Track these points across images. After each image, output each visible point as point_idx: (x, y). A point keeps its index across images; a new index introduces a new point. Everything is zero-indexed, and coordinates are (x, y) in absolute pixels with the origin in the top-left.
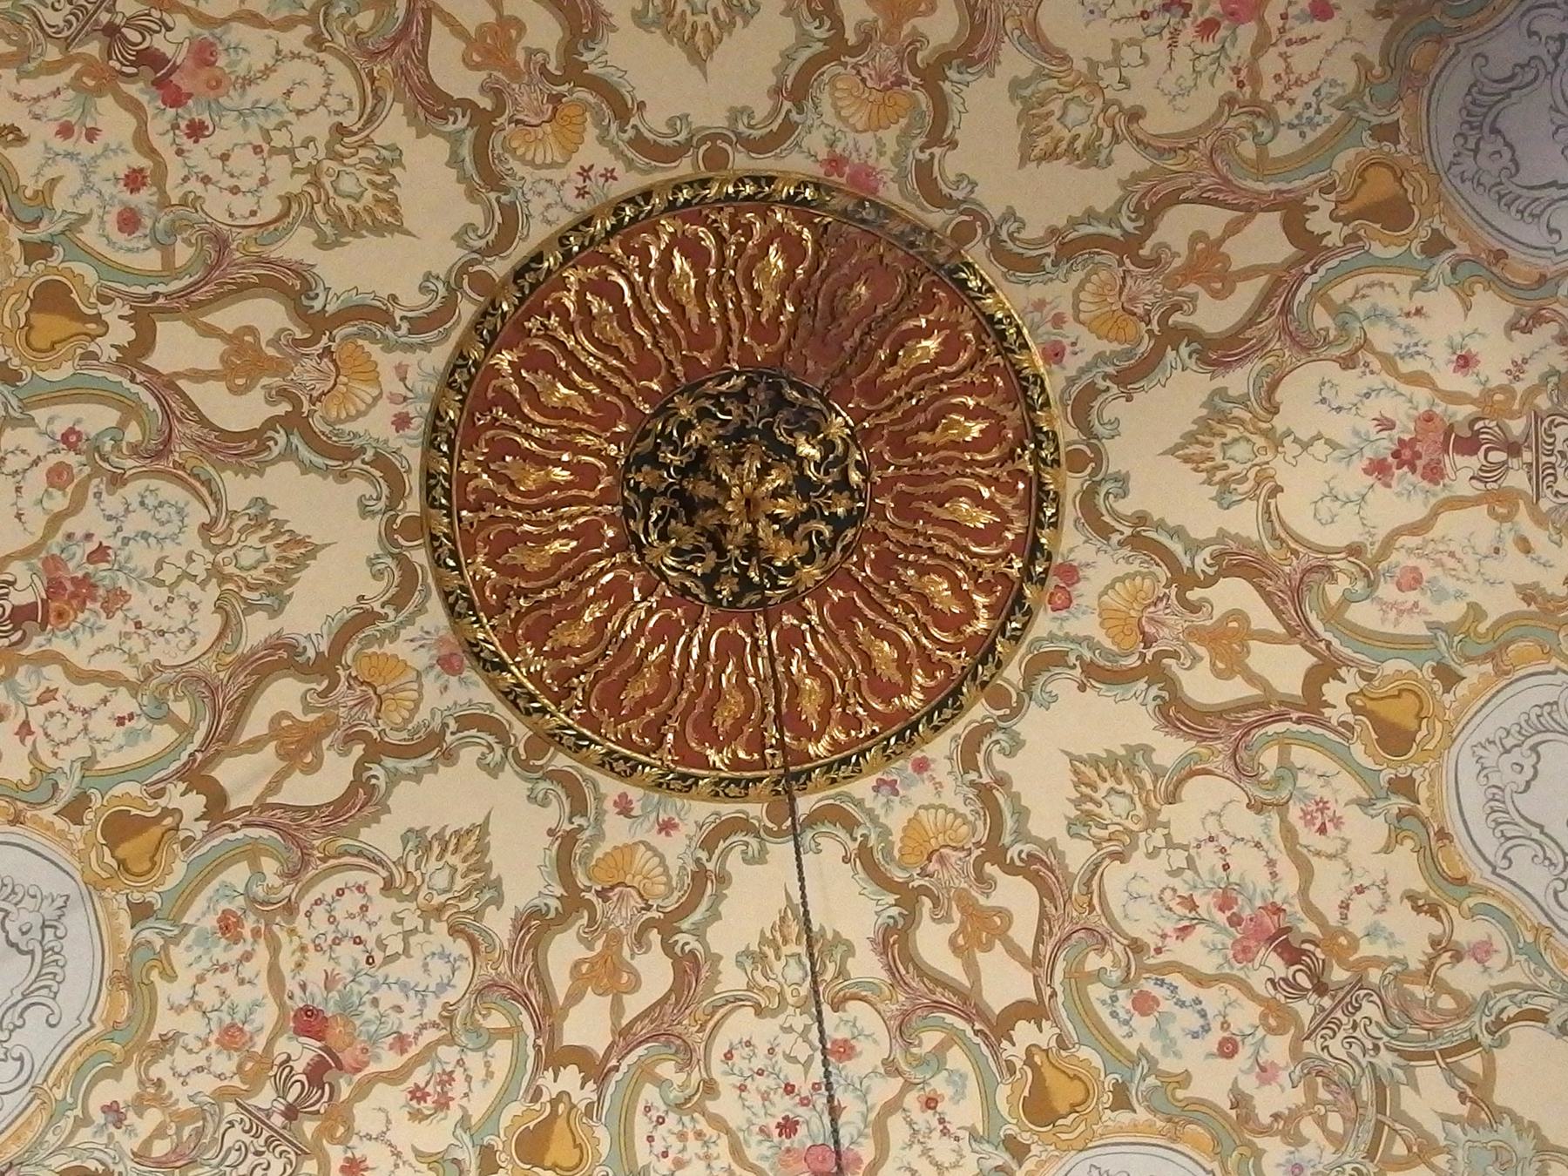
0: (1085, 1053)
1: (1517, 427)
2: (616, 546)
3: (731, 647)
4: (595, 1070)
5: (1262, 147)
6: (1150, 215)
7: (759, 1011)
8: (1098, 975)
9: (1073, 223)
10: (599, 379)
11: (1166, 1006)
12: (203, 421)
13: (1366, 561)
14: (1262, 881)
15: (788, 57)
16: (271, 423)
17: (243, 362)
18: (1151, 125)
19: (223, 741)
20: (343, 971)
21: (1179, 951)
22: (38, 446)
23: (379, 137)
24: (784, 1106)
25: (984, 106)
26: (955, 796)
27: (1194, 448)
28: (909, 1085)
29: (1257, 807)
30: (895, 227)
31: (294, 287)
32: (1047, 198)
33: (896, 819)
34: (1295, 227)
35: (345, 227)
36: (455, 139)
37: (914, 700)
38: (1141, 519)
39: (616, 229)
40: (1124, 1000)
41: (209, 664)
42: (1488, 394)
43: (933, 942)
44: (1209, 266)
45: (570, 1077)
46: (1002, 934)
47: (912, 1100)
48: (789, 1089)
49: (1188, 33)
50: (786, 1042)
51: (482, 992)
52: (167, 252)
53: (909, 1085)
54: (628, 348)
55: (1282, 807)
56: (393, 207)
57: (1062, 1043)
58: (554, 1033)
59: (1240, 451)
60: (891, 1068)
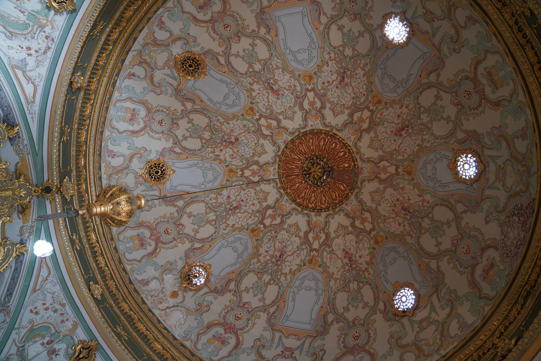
0: (261, 234)
1: (354, 266)
2: (305, 158)
3: (298, 175)
4: (242, 175)
5: (380, 222)
6: (367, 211)
7: (255, 193)
8: (271, 233)
9: (364, 201)
10: (325, 148)
11: (270, 243)
12: (303, 101)
13: (332, 252)
14: (288, 250)
15: (373, 158)
16: (306, 110)
17: (312, 104)
18: (379, 207)
19: (266, 118)
20: (244, 141)
21: (277, 242)
22: (293, 83)
23: (345, 110)
24: (245, 199)
25: (374, 185)
26: (288, 209)
27: (340, 226)
28: (251, 214)
29: (297, 247)
30: (356, 179)
31: (323, 107)
32: (366, 197)
33: (283, 203)
34: (372, 230)
35: (333, 110)
36: (348, 120)
37: (298, 201)
38: (329, 222)
39: (344, 144)
40: (269, 237)
41: (275, 113)
42: (357, 261)
43: (270, 212)
44: (364, 220)
45: (240, 173)
46: (273, 220)
47: (250, 215)
48: (247, 200)
49: (392, 208)
50: (252, 197)
51: (247, 159)
52: (322, 89)
53: (251, 214)
54: (330, 150)
55: (298, 250)
56: (337, 115)
57: (262, 231)
58: (245, 169)
59: (341, 232)
60: (253, 211)
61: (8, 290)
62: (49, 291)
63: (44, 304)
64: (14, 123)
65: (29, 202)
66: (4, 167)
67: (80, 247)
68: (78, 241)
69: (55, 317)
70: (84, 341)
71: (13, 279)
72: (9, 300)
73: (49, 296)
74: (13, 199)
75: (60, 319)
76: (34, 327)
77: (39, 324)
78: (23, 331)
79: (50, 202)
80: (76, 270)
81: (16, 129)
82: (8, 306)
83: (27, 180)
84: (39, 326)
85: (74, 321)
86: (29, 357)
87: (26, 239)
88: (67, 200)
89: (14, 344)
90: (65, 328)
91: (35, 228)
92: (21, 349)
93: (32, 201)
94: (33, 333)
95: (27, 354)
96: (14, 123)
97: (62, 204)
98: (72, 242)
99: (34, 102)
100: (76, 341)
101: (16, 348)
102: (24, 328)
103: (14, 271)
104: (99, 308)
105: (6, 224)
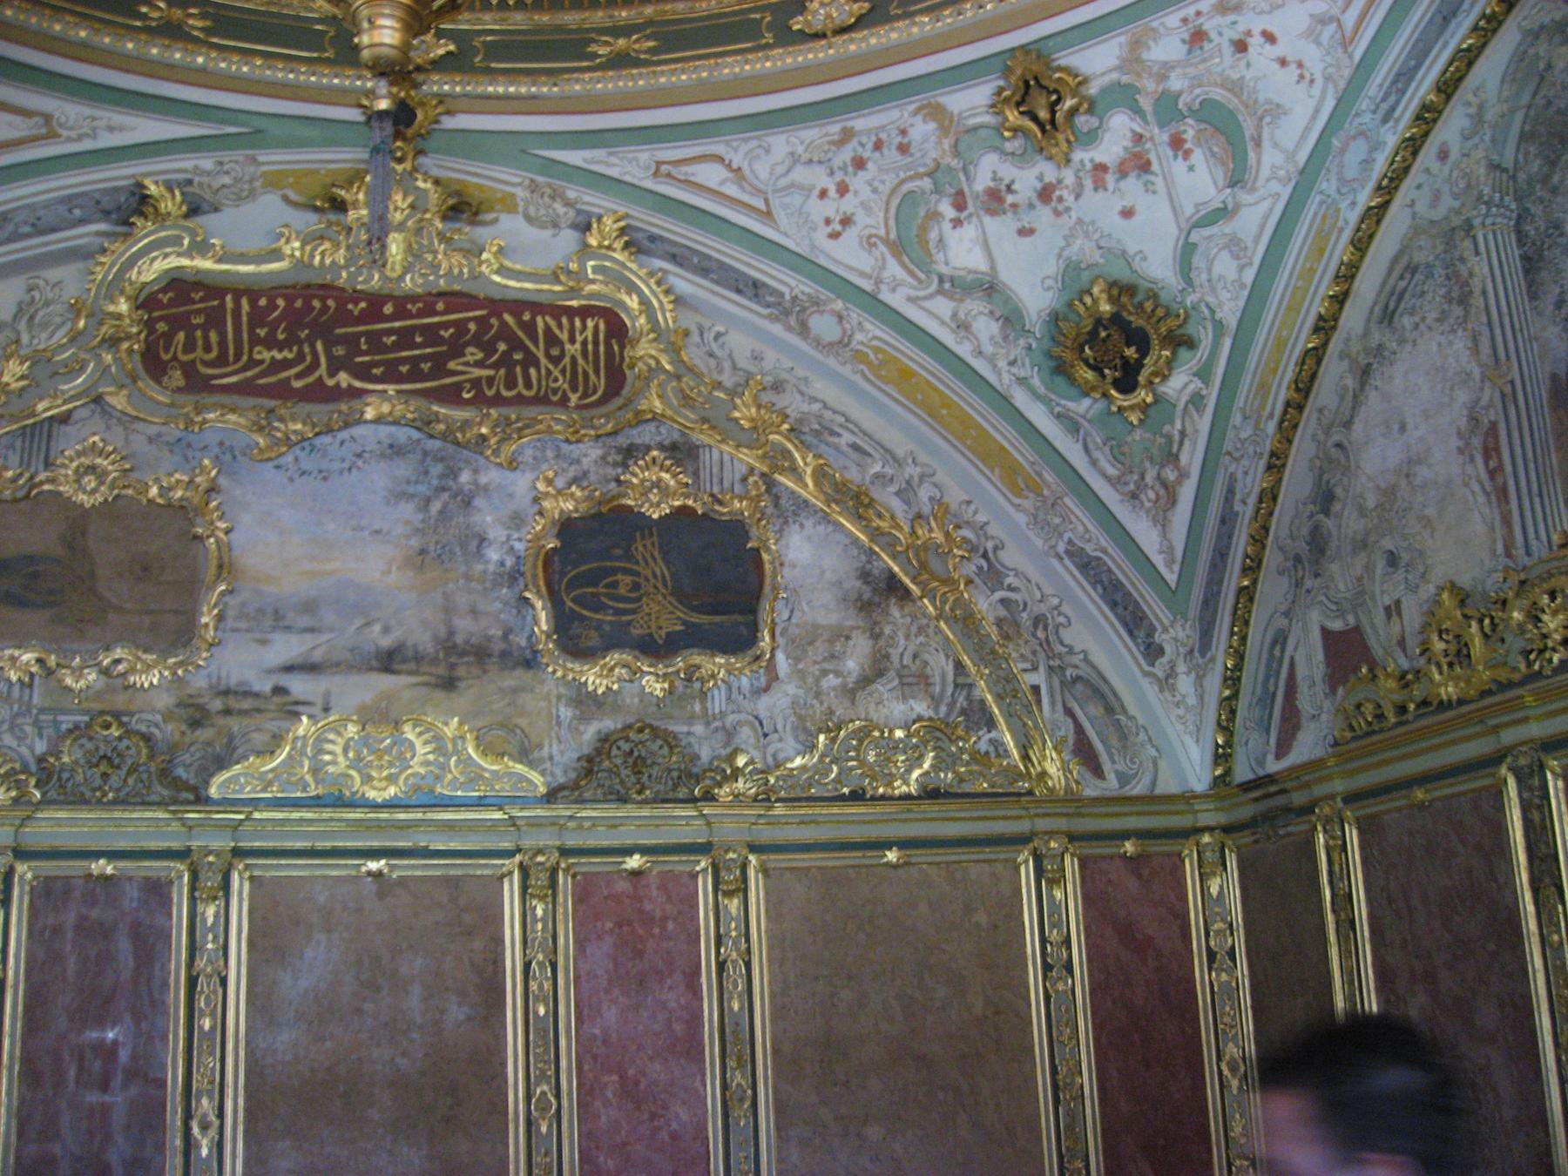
61: (739, 291)
62: (780, 170)
63: (823, 194)
64: (133, 194)
65: (437, 182)
66: (297, 244)
67: (648, 38)
68: (621, 42)
69: (880, 170)
70: (1000, 90)
71: (704, 272)
72: (774, 292)
73: (800, 174)
74: (419, 231)
75: (891, 154)
76: (893, 236)
77: (886, 220)
78: (894, 269)
79: (449, 113)
80: (732, 68)
81: (153, 189)
82: (795, 299)
83: (354, 178)
84: (892, 222)
85: (916, 112)
86: (983, 267)
87: (572, 213)
88: (449, 53)
89: (927, 304)
90: (930, 146)
91: (540, 179)
92: (947, 286)
93: (435, 172)
94: (910, 241)
95: (970, 272)
96: (133, 194)
97: (460, 70)
98: (621, 61)
99: (47, 118)
100: (988, 119)
101: (940, 300)
102: (883, 268)
103: (681, 265)
104: (899, 18)
105: (508, 263)
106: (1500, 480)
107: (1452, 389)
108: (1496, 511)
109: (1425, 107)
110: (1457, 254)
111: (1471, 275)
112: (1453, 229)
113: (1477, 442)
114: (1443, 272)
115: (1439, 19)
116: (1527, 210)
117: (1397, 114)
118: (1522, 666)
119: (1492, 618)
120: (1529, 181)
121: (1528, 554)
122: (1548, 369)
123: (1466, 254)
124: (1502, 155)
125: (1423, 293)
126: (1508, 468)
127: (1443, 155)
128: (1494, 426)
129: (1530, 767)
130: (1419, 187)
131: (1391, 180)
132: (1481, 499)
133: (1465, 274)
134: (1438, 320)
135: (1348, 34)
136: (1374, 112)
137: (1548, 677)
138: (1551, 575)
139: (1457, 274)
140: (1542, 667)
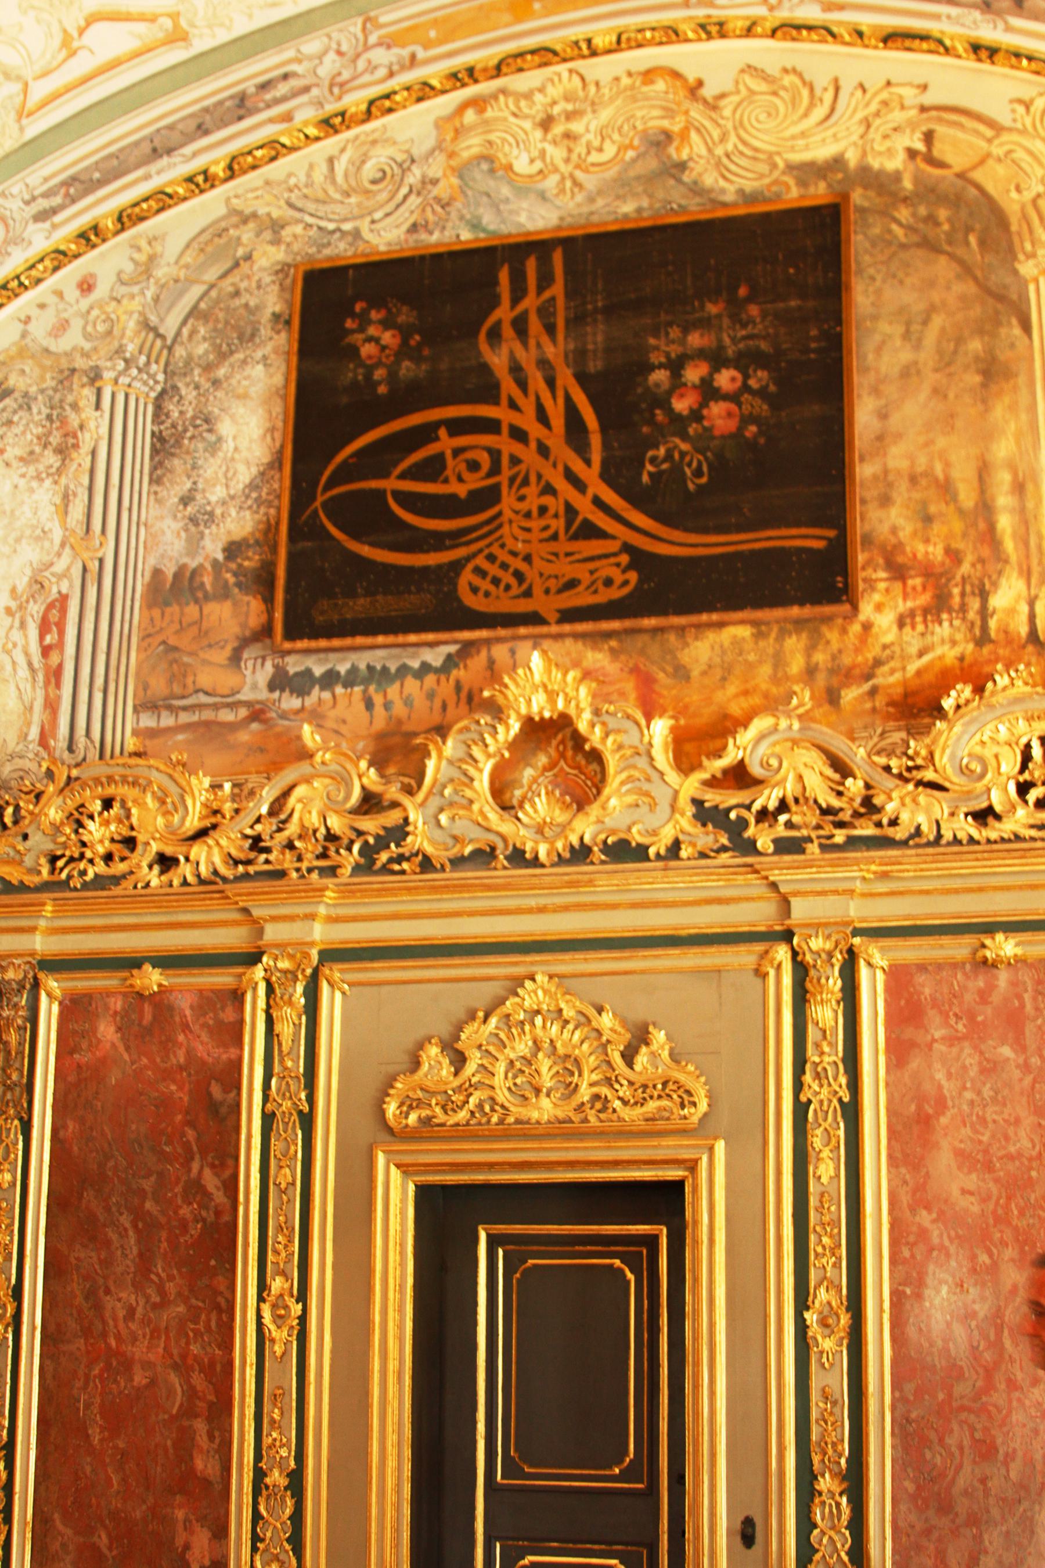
106: (54, 659)
107: (18, 540)
108: (40, 694)
109: (95, 229)
110: (70, 399)
111: (81, 427)
112: (73, 371)
113: (36, 609)
114: (46, 411)
115: (146, 148)
116: (175, 388)
117: (58, 219)
118: (45, 871)
119: (17, 808)
120: (189, 360)
121: (71, 749)
122: (152, 561)
123: (82, 404)
124: (162, 320)
125: (9, 423)
126: (70, 649)
127: (86, 286)
128: (64, 599)
129: (19, 983)
130: (42, 306)
131: (21, 284)
132: (23, 672)
133: (76, 424)
134: (21, 459)
135: (30, 105)
136: (27, 203)
137: (76, 889)
138: (110, 779)
139: (63, 421)
140: (70, 877)
